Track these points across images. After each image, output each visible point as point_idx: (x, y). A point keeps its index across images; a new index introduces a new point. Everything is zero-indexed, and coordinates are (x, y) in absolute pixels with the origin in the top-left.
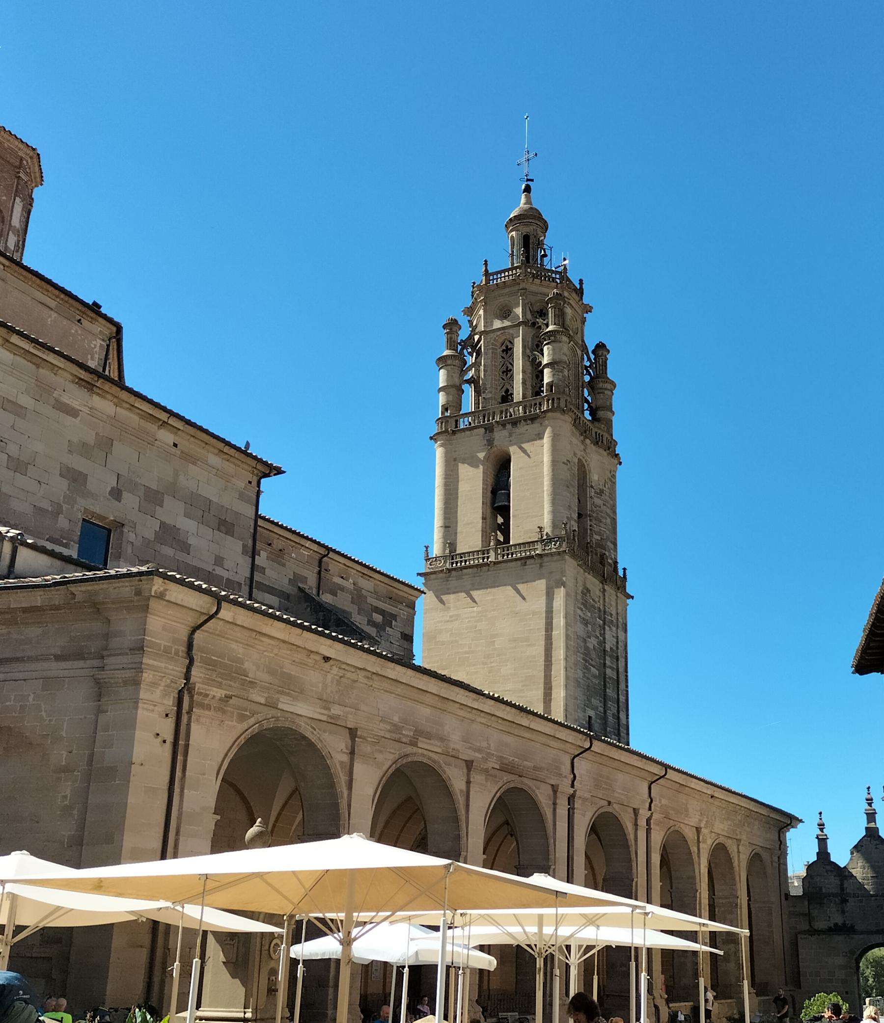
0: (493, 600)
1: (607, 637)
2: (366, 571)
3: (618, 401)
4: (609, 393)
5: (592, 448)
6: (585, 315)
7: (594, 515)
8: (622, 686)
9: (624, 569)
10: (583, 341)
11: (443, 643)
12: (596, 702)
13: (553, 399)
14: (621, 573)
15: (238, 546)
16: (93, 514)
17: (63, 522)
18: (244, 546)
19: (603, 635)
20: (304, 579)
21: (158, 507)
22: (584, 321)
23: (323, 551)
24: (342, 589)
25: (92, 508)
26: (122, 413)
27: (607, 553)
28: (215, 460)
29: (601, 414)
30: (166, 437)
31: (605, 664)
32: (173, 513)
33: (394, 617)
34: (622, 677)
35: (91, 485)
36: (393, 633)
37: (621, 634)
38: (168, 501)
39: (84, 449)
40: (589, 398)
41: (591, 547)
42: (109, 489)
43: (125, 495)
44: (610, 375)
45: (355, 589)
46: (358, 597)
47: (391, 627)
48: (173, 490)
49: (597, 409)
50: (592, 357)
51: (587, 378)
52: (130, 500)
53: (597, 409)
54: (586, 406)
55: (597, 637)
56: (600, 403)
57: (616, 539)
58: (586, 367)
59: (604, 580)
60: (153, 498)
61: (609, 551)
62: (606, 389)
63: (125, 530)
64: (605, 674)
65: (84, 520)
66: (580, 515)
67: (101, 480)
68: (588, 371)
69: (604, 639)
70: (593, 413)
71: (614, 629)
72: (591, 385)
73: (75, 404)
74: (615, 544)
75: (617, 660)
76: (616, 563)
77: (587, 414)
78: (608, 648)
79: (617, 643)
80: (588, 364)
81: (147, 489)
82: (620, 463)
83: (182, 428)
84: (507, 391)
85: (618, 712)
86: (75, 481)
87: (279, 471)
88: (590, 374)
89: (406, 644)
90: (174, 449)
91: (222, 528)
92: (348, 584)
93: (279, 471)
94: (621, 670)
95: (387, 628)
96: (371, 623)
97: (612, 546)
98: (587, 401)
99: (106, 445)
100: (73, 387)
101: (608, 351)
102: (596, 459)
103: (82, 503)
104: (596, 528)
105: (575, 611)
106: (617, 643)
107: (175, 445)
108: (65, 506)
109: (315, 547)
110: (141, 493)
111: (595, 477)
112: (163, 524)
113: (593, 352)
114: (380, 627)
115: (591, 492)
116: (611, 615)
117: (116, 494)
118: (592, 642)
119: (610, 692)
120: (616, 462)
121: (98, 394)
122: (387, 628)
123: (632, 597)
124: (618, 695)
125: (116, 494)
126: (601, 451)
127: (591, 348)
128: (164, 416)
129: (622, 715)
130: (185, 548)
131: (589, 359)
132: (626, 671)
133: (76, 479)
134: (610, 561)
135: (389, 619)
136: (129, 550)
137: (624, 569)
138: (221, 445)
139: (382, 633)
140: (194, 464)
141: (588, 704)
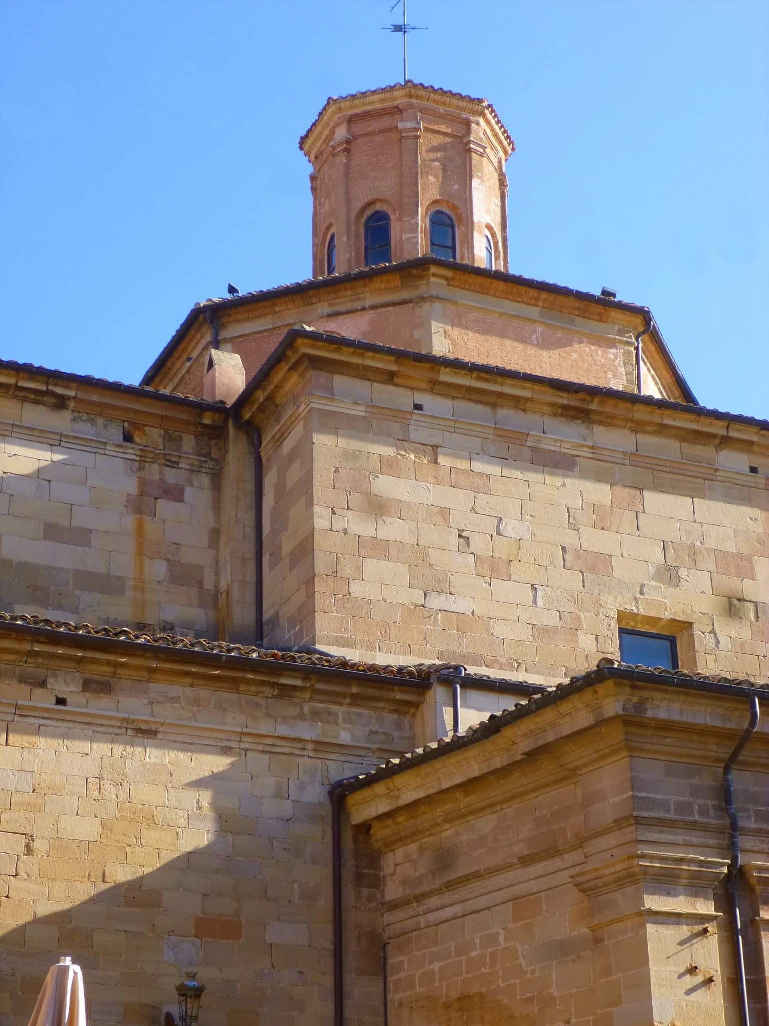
16: (633, 616)
43: (683, 573)
63: (697, 632)
65: (622, 631)
73: (566, 449)
81: (721, 556)
83: (755, 438)
90: (751, 478)
100: (551, 423)
103: (613, 604)
107: (753, 470)
110: (712, 566)
117: (669, 575)
125: (669, 575)
128: (718, 428)
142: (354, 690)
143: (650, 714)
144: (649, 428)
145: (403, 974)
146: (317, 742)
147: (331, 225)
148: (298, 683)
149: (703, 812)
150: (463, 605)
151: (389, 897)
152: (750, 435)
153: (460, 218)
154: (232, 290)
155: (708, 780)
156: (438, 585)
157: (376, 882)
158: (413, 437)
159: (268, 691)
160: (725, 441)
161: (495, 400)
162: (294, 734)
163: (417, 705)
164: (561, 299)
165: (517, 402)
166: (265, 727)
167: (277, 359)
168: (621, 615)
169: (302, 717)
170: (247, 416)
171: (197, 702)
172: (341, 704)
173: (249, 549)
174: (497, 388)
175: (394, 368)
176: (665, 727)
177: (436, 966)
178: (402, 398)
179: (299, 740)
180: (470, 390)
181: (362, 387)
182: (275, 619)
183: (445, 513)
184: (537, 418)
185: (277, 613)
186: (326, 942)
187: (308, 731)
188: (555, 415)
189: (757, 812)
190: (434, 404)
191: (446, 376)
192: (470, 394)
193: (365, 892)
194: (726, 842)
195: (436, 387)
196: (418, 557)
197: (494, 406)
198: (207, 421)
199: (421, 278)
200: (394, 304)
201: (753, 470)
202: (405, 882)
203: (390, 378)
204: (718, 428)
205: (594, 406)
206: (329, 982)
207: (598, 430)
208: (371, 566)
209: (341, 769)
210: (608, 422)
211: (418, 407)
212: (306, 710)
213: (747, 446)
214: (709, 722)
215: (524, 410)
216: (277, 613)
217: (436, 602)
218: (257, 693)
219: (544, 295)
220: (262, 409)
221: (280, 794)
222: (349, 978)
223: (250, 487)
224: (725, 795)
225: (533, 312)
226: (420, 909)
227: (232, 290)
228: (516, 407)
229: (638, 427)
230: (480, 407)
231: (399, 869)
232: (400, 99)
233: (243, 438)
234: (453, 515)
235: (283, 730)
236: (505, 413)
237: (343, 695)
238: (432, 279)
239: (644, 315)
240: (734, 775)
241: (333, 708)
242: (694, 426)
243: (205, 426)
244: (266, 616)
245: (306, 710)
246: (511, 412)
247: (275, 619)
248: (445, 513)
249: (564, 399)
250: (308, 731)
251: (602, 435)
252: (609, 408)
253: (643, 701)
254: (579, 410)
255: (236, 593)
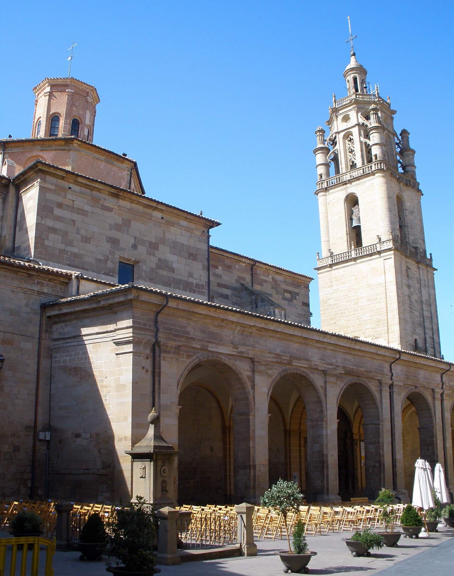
0: (356, 279)
1: (423, 293)
2: (278, 271)
3: (418, 160)
4: (412, 156)
5: (404, 188)
6: (393, 116)
7: (409, 225)
8: (434, 320)
9: (431, 254)
10: (394, 130)
11: (331, 305)
12: (419, 330)
13: (378, 164)
14: (428, 257)
15: (200, 266)
16: (124, 258)
17: (110, 265)
18: (203, 265)
19: (420, 292)
20: (244, 279)
21: (156, 251)
22: (392, 119)
23: (252, 263)
24: (266, 281)
25: (123, 256)
26: (134, 206)
27: (419, 246)
28: (184, 223)
29: (408, 168)
30: (157, 215)
31: (423, 309)
32: (165, 253)
33: (297, 294)
34: (434, 315)
35: (122, 245)
36: (297, 302)
37: (431, 292)
38: (161, 247)
39: (117, 227)
40: (401, 160)
41: (409, 243)
42: (131, 245)
43: (139, 246)
44: (412, 146)
45: (273, 281)
46: (275, 284)
47: (296, 299)
48: (163, 241)
49: (406, 166)
50: (400, 137)
51: (398, 150)
52: (142, 249)
53: (406, 166)
54: (399, 165)
55: (417, 294)
56: (407, 163)
57: (424, 238)
58: (397, 144)
59: (418, 262)
60: (154, 246)
61: (421, 245)
62: (410, 154)
64: (423, 314)
66: (400, 226)
67: (126, 240)
68: (398, 146)
69: (421, 295)
70: (404, 168)
71: (427, 288)
72: (401, 153)
73: (110, 205)
74: (424, 240)
75: (430, 306)
76: (425, 251)
77: (401, 170)
78: (424, 298)
79: (430, 296)
80: (398, 142)
81: (150, 243)
82: (423, 195)
84: (353, 162)
85: (433, 335)
86: (114, 243)
87: (218, 224)
88: (400, 147)
89: (305, 308)
90: (162, 220)
91: (191, 257)
92: (270, 279)
93: (218, 224)
94: (433, 311)
95: (294, 301)
96: (284, 299)
97: (422, 242)
98: (400, 162)
99: (127, 223)
100: (107, 197)
101: (409, 134)
102: (408, 194)
103: (118, 255)
104: (410, 233)
105: (401, 281)
106: (430, 296)
107: (162, 218)
108: (110, 256)
109: (248, 261)
111: (408, 204)
112: (160, 260)
113: (400, 135)
114: (290, 300)
115: (407, 213)
116: (425, 281)
118: (415, 297)
119: (427, 324)
120: (420, 194)
121: (122, 199)
122: (294, 301)
123: (437, 270)
124: (432, 325)
125: (134, 247)
126: (410, 188)
127: (398, 132)
128: (155, 205)
129: (435, 337)
130: (173, 270)
131: (398, 139)
132: (436, 312)
133: (114, 242)
134: (421, 250)
135: (294, 295)
136: (144, 274)
137: (431, 254)
138: (186, 215)
139: (291, 303)
140: (173, 226)
141: (414, 332)
142: (50, 277)
143: (140, 299)
144: (135, 202)
145: (57, 359)
146: (38, 291)
147: (41, 117)
148: (35, 274)
149: (150, 326)
150: (75, 250)
151: (54, 337)
152: (163, 208)
153: (82, 122)
154: (10, 136)
155: (152, 317)
156: (70, 243)
157: (51, 333)
158: (67, 197)
159: (26, 275)
160: (155, 209)
161: (92, 189)
162: (32, 288)
163: (67, 283)
164: (111, 155)
165: (99, 190)
166: (24, 285)
167: (31, 168)
168: (121, 257)
169: (34, 284)
170: (16, 183)
171: (5, 276)
172: (45, 281)
173: (12, 224)
174: (94, 185)
175: (65, 176)
176: (144, 302)
177: (68, 358)
178: (66, 184)
179: (33, 290)
180: (86, 185)
181: (54, 180)
182: (19, 247)
183: (74, 222)
184: (104, 195)
185: (20, 246)
186: (36, 348)
187: (36, 288)
188: (109, 195)
189: (163, 327)
190: (75, 187)
191: (80, 180)
192: (85, 186)
193: (47, 335)
194: (155, 334)
195: (76, 182)
196: (65, 234)
197: (92, 190)
198: (3, 182)
199: (71, 143)
200: (61, 150)
201: (162, 218)
202: (60, 334)
203: (63, 178)
204: (155, 205)
205: (121, 194)
206: (36, 360)
207: (121, 201)
208: (51, 236)
209: (45, 300)
210: (124, 199)
211: (70, 188)
212: (36, 281)
213: (161, 211)
214: (155, 302)
215: (100, 193)
216: (20, 246)
217: (69, 249)
218: (22, 276)
219: (107, 153)
220: (22, 182)
221: (27, 305)
222: (42, 359)
223: (14, 204)
224: (156, 322)
225: (103, 158)
226: (65, 342)
227: (10, 136)
228: (98, 191)
229: (132, 201)
230: (88, 190)
231: (58, 330)
232: (68, 83)
233: (14, 188)
234: (76, 222)
235: (29, 287)
236: (94, 193)
237: (47, 278)
238: (74, 144)
239: (135, 164)
240: (160, 316)
241: (43, 281)
242: (148, 203)
243: (3, 184)
244: (16, 245)
245: (36, 281)
246: (96, 193)
247: (19, 247)
248: (74, 222)
249: (113, 191)
250: (36, 288)
251: (121, 202)
252: (125, 195)
253: (139, 295)
254: (116, 194)
255: (7, 237)
